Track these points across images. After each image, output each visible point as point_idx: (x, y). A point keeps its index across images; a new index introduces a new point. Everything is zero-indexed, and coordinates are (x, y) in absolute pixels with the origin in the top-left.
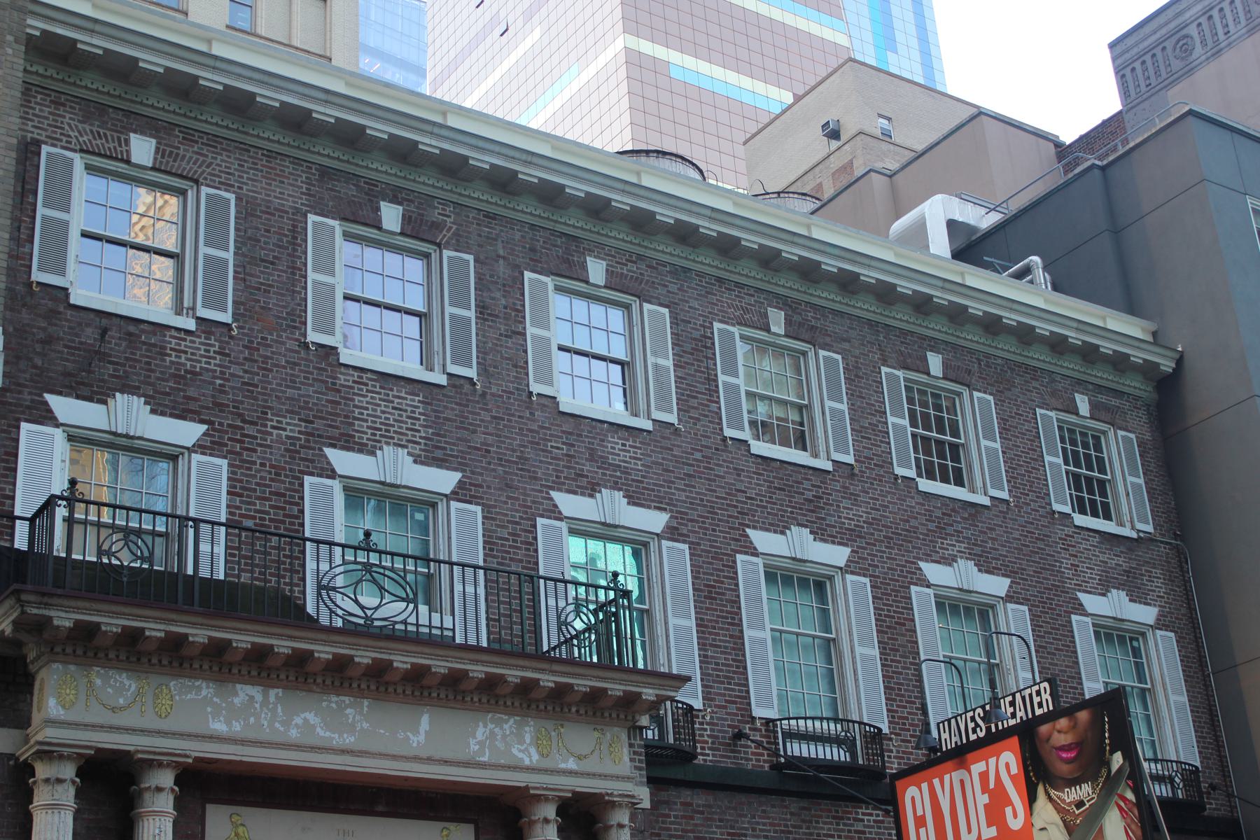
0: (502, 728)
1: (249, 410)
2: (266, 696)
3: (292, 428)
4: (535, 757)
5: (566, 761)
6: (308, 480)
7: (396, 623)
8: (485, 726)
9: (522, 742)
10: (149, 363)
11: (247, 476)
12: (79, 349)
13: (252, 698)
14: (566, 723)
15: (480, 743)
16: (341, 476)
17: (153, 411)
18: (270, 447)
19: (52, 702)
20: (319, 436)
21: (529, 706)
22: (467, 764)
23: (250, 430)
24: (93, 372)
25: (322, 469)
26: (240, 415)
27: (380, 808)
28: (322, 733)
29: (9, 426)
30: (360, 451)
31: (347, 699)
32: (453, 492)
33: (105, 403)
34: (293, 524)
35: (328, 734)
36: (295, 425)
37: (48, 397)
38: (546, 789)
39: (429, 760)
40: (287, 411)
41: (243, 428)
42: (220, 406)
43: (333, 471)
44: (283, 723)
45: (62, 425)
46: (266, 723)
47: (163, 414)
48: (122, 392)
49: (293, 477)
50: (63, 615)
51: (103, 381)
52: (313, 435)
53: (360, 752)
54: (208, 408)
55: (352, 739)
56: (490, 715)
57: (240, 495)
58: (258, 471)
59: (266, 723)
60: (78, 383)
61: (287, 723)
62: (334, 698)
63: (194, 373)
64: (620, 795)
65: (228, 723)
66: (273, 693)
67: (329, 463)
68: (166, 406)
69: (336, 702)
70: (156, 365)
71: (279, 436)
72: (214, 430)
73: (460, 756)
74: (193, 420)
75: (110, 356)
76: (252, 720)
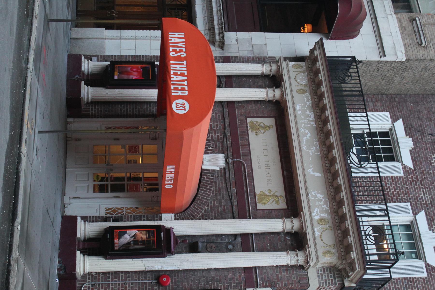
0: (324, 204)
1: (426, 182)
2: (312, 121)
3: (427, 198)
4: (317, 218)
5: (318, 231)
6: (408, 204)
7: (350, 159)
8: (323, 198)
9: (321, 212)
10: (427, 149)
11: (401, 183)
12: (421, 128)
13: (310, 117)
14: (333, 231)
15: (316, 196)
16: (415, 217)
17: (410, 151)
18: (415, 191)
19: (293, 63)
20: (428, 209)
21: (335, 212)
22: (306, 189)
23: (418, 183)
24: (415, 132)
25: (415, 210)
26: (422, 179)
27: (285, 173)
28: (305, 138)
29: (386, 110)
30: (429, 225)
31: (318, 147)
32: (428, 264)
33: (407, 135)
34: (390, 200)
35: (305, 141)
36: (428, 199)
37: (401, 120)
38: (304, 218)
39: (304, 175)
40: (432, 197)
41: (418, 181)
42: (423, 173)
43: (416, 214)
44: (304, 126)
45: (393, 125)
46: (303, 121)
47: (411, 154)
48: (413, 140)
49: (407, 199)
50: (318, 52)
51: (414, 135)
52: (427, 206)
53: (301, 151)
54: (420, 168)
55: (305, 149)
56: (327, 200)
57: (393, 181)
58: (404, 187)
59: (303, 121)
60: (410, 128)
61: (304, 127)
62: (317, 143)
63: (431, 163)
64: (309, 251)
65: (300, 110)
66: (314, 123)
67: (418, 213)
68: (414, 155)
69: (316, 144)
70: (428, 151)
71: (421, 194)
72: (413, 171)
73: (309, 187)
74: (413, 164)
75: (424, 137)
76: (303, 117)
